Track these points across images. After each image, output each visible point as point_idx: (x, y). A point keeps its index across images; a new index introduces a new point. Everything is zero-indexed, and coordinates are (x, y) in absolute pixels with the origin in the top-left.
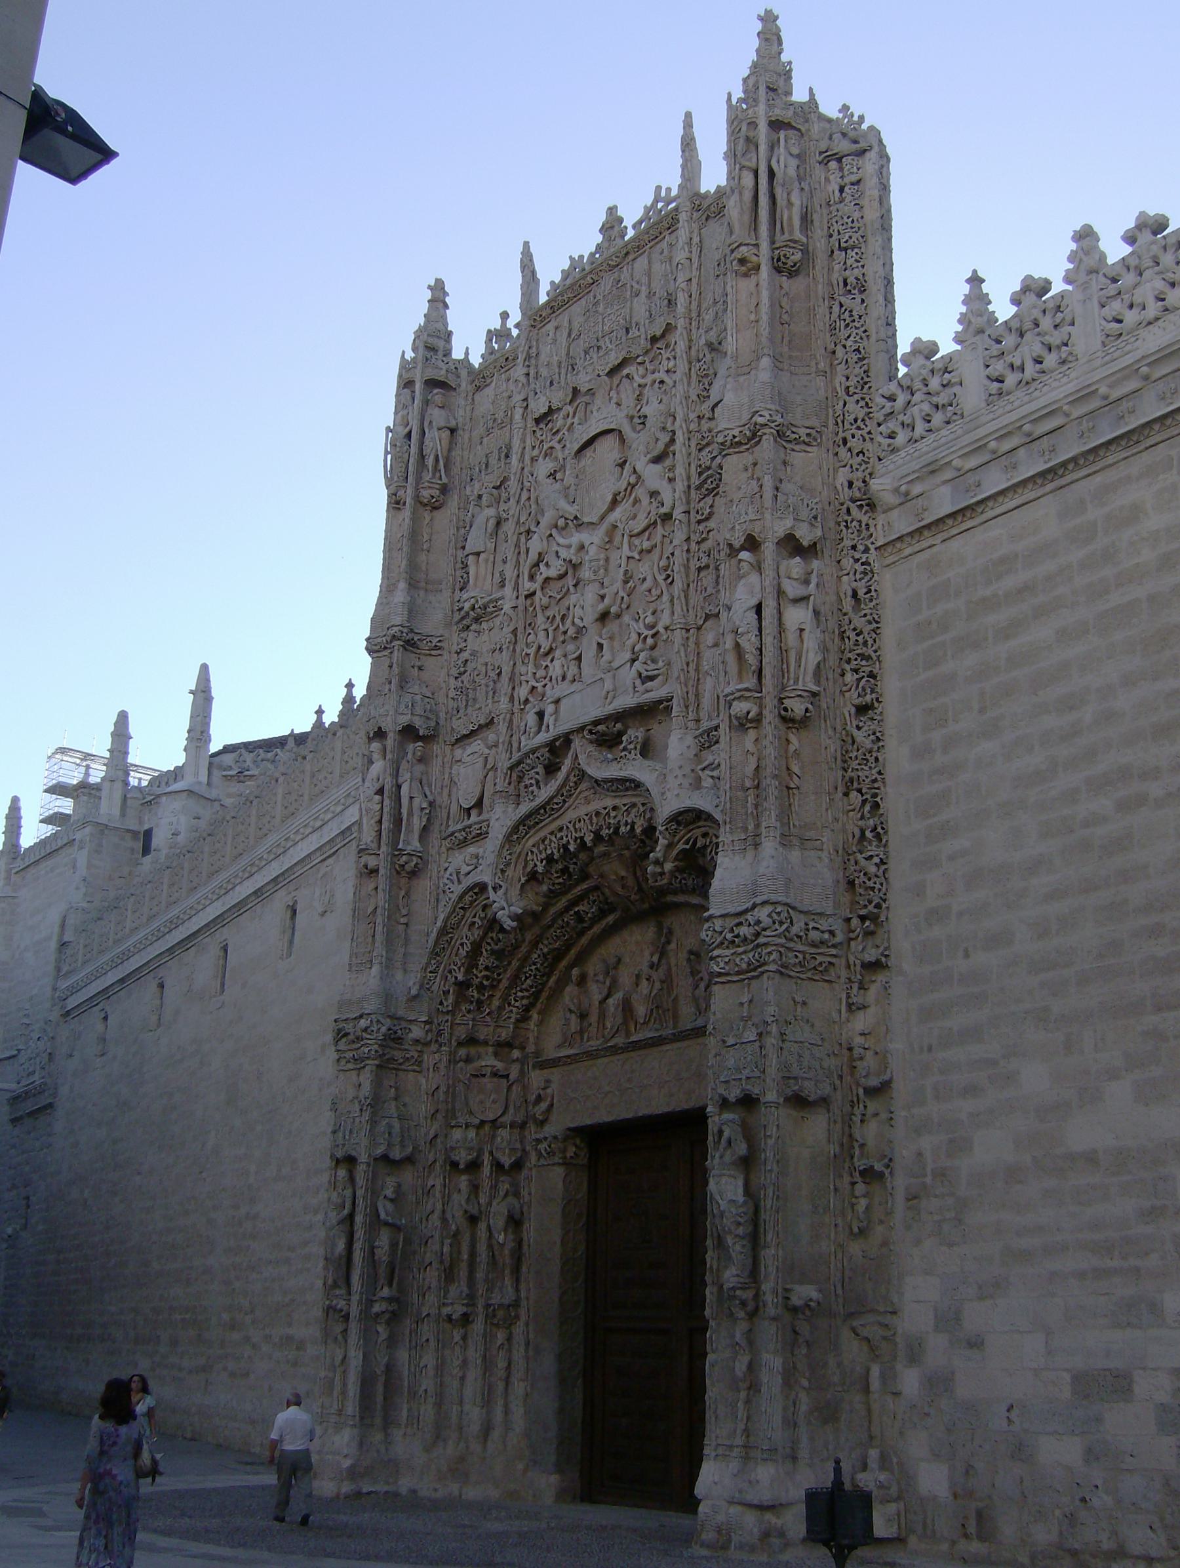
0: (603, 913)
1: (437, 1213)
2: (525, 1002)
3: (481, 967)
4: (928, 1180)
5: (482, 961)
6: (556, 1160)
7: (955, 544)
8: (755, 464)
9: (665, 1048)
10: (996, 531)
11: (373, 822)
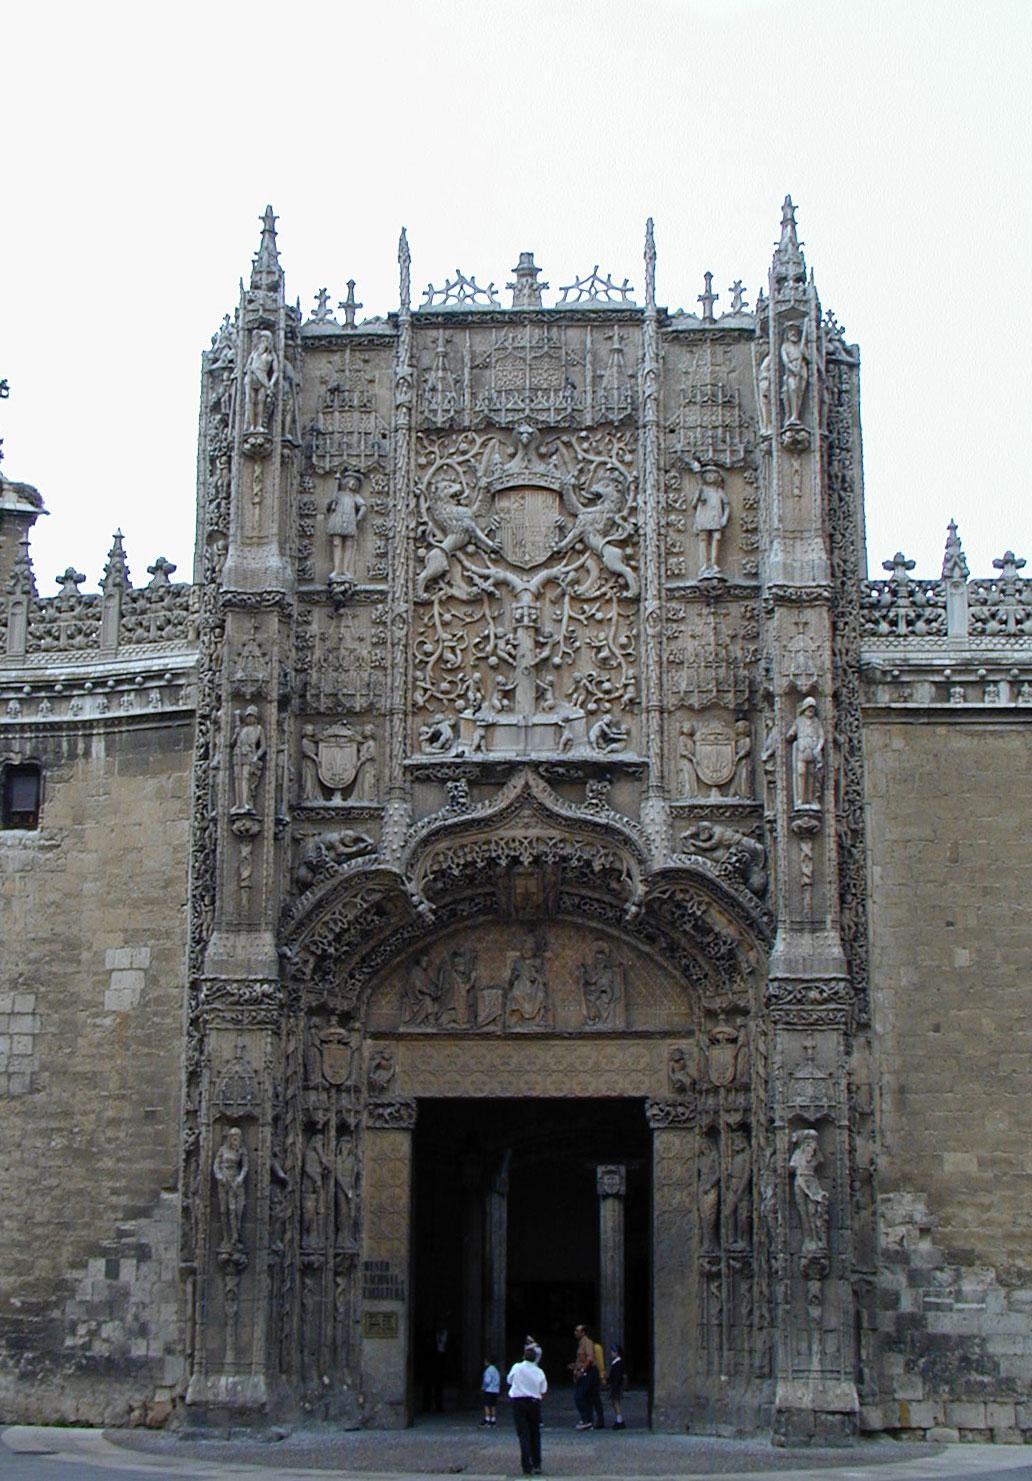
1: (298, 1170)
6: (404, 1125)
8: (806, 624)
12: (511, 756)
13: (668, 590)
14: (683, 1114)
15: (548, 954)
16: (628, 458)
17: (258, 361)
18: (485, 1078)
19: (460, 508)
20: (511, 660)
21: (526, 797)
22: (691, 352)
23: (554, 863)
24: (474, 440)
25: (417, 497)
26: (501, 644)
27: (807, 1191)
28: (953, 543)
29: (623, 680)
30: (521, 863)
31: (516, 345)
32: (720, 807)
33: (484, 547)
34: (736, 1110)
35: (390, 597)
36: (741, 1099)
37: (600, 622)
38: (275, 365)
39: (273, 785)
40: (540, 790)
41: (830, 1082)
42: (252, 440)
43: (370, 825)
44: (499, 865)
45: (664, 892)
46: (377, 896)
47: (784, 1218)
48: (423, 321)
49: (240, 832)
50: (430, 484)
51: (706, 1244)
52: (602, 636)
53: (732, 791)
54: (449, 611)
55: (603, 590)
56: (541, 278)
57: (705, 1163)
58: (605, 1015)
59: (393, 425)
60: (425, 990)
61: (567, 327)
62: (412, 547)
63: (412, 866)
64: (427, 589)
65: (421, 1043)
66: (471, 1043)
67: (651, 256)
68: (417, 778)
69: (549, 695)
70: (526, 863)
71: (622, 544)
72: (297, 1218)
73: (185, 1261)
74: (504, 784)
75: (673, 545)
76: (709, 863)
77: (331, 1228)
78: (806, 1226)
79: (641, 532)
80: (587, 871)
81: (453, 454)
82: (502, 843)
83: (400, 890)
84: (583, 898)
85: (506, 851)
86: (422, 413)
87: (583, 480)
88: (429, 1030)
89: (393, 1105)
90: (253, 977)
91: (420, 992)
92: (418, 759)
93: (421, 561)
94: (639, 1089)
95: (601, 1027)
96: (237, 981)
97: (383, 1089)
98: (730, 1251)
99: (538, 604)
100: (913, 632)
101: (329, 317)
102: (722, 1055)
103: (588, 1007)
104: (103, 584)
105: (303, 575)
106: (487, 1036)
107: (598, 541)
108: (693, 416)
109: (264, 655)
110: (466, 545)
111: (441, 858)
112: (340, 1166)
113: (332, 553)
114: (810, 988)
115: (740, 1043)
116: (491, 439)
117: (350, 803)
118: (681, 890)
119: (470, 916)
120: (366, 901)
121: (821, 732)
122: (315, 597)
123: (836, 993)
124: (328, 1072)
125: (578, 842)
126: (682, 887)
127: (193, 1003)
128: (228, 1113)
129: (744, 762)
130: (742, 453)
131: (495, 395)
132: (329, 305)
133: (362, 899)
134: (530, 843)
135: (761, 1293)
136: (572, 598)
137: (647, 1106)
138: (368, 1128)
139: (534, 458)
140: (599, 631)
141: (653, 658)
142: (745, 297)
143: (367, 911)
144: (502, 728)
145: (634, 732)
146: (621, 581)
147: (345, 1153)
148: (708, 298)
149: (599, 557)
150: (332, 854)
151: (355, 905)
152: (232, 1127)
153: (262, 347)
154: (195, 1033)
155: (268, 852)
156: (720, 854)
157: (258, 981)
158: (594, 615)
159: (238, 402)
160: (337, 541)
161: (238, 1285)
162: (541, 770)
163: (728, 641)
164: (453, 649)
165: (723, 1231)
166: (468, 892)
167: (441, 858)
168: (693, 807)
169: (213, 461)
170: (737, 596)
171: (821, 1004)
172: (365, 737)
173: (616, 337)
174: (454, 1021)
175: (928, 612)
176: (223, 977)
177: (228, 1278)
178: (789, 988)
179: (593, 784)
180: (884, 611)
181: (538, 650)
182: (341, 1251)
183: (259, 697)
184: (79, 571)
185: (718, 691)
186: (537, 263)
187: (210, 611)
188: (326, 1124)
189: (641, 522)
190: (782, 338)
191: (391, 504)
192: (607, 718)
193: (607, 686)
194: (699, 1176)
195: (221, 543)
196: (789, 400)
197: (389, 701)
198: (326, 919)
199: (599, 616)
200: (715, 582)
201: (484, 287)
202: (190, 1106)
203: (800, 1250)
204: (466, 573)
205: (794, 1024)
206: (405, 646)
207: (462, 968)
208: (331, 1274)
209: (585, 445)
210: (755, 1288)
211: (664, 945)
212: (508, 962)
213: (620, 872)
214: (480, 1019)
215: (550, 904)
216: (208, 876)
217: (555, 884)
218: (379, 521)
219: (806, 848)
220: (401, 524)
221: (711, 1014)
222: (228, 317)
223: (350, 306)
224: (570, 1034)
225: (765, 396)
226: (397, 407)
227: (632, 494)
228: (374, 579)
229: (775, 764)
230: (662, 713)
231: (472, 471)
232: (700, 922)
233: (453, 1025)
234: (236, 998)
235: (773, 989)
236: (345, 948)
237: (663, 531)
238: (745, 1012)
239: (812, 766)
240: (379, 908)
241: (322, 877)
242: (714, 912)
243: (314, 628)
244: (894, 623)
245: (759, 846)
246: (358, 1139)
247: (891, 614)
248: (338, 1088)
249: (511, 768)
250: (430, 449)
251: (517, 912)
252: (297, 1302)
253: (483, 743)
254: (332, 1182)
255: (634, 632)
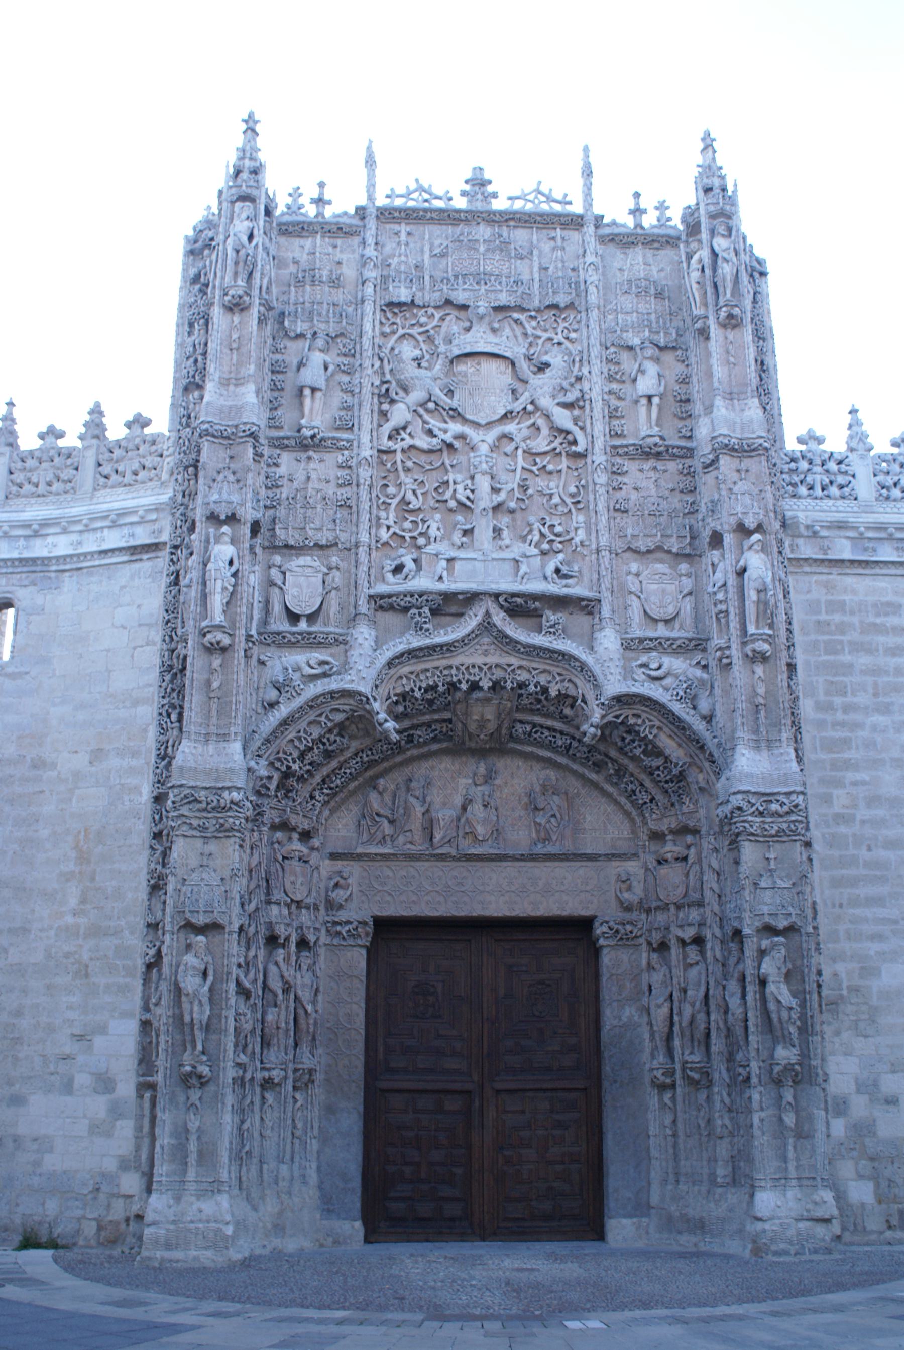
0: (435, 739)
2: (326, 798)
3: (306, 762)
4: (845, 992)
5: (309, 757)
6: (359, 942)
7: (849, 581)
8: (747, 471)
9: (504, 864)
10: (882, 584)
11: (225, 601)
12: (472, 586)
13: (614, 447)
14: (631, 932)
15: (497, 782)
16: (573, 335)
17: (241, 227)
18: (442, 899)
19: (422, 371)
20: (469, 503)
21: (487, 625)
22: (625, 253)
23: (512, 689)
24: (433, 315)
25: (381, 360)
26: (460, 488)
27: (780, 998)
28: (854, 424)
29: (575, 524)
30: (480, 689)
31: (470, 238)
32: (668, 639)
33: (442, 404)
34: (689, 925)
35: (355, 444)
36: (694, 914)
37: (550, 473)
38: (256, 232)
39: (244, 601)
40: (499, 618)
41: (794, 890)
42: (231, 292)
43: (335, 649)
44: (459, 689)
45: (617, 717)
46: (339, 717)
47: (757, 1026)
48: (387, 215)
49: (212, 644)
50: (393, 349)
51: (661, 1059)
52: (552, 485)
53: (677, 626)
54: (410, 459)
55: (553, 446)
56: (490, 189)
57: (657, 978)
58: (554, 838)
59: (359, 297)
60: (382, 812)
61: (515, 227)
62: (376, 400)
63: (377, 687)
64: (390, 438)
65: (378, 864)
66: (427, 864)
67: (588, 172)
68: (381, 607)
69: (505, 533)
70: (486, 688)
71: (569, 406)
72: (258, 1032)
73: (143, 1076)
74: (461, 615)
75: (616, 410)
76: (661, 690)
77: (291, 1041)
78: (779, 1033)
79: (587, 397)
80: (543, 698)
81: (413, 325)
82: (463, 668)
83: (365, 710)
84: (534, 726)
85: (467, 676)
86: (387, 289)
87: (532, 352)
88: (386, 851)
89: (350, 923)
90: (220, 785)
91: (377, 814)
92: (382, 589)
93: (384, 414)
94: (587, 908)
95: (550, 849)
96: (206, 788)
97: (341, 907)
98: (687, 1062)
99: (494, 455)
100: (828, 496)
101: (303, 211)
102: (672, 875)
103: (538, 832)
104: (82, 438)
105: (272, 421)
106: (442, 857)
107: (545, 402)
108: (628, 302)
109: (238, 481)
110: (426, 403)
111: (404, 681)
112: (299, 982)
113: (301, 404)
114: (771, 801)
115: (690, 861)
116: (448, 314)
117: (313, 629)
118: (634, 715)
119: (425, 743)
120: (330, 720)
121: (769, 566)
122: (286, 442)
123: (796, 806)
124: (288, 886)
125: (535, 669)
126: (635, 712)
127: (157, 817)
128: (193, 921)
129: (688, 599)
130: (674, 335)
131: (452, 279)
132: (301, 201)
133: (327, 717)
134: (490, 668)
135: (722, 1101)
136: (524, 452)
137: (596, 924)
138: (325, 945)
139: (488, 331)
140: (550, 481)
141: (601, 506)
142: (668, 214)
143: (330, 731)
144: (463, 562)
145: (585, 571)
146: (570, 437)
147: (304, 968)
148: (637, 212)
149: (548, 416)
150: (296, 676)
151: (320, 723)
152: (197, 935)
153: (244, 216)
154: (157, 847)
155: (239, 664)
156: (668, 681)
157: (228, 788)
158: (544, 467)
159: (219, 266)
160: (307, 392)
161: (200, 1099)
162: (501, 599)
163: (667, 493)
164: (414, 492)
165: (677, 1042)
166: (427, 718)
167: (404, 681)
168: (641, 640)
169: (191, 325)
170: (674, 455)
171: (781, 816)
172: (330, 569)
173: (559, 237)
174: (411, 843)
175: (841, 480)
176: (192, 783)
177: (191, 1092)
178: (753, 801)
179: (551, 616)
180: (802, 476)
181: (494, 496)
182: (300, 1066)
183: (232, 519)
184: (58, 427)
185: (662, 536)
186: (487, 176)
187: (185, 452)
188: (287, 939)
189: (586, 386)
190: (713, 233)
191: (358, 364)
192: (561, 556)
193: (558, 529)
194: (650, 990)
195: (196, 394)
196: (724, 280)
197: (354, 536)
198: (290, 736)
199: (550, 467)
200: (657, 440)
201: (440, 193)
202: (151, 919)
203: (772, 1056)
204: (427, 426)
205: (757, 835)
206: (371, 487)
207: (417, 793)
208: (290, 1089)
209: (534, 323)
210: (717, 1098)
211: (612, 771)
212: (460, 788)
213: (575, 699)
214: (435, 841)
215: (504, 731)
216: (175, 695)
217: (511, 709)
218: (345, 378)
219: (759, 670)
220: (368, 380)
221: (657, 837)
222: (209, 208)
223: (320, 201)
224: (523, 855)
225: (698, 283)
226: (363, 283)
227: (577, 365)
228: (338, 429)
229: (726, 592)
230: (610, 553)
231: (430, 340)
232: (650, 747)
233: (409, 846)
234: (204, 805)
235: (737, 800)
236: (308, 767)
237: (606, 397)
238: (695, 832)
239: (762, 595)
240: (341, 728)
241: (289, 695)
242: (662, 736)
243: (282, 470)
244: (811, 488)
245: (705, 676)
246: (316, 955)
247: (809, 479)
248: (299, 904)
249: (471, 598)
250: (392, 320)
251: (470, 739)
252: (257, 1117)
253: (445, 574)
254: (292, 996)
255: (583, 482)
